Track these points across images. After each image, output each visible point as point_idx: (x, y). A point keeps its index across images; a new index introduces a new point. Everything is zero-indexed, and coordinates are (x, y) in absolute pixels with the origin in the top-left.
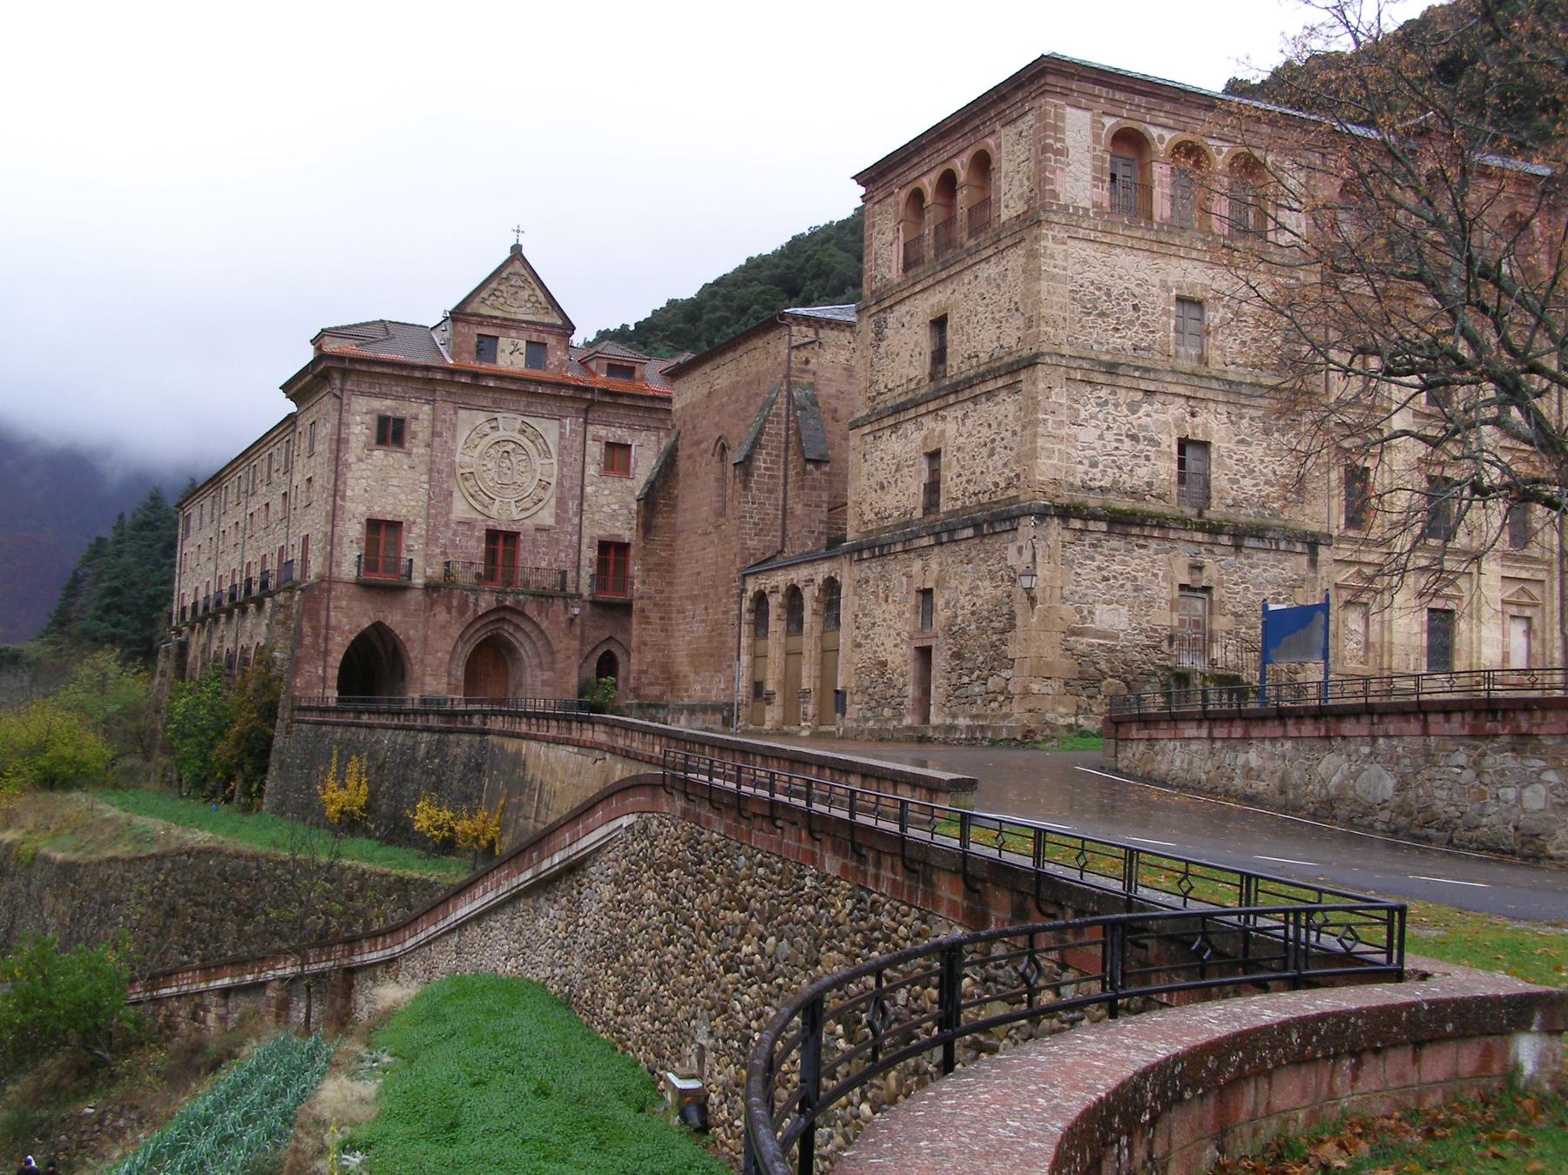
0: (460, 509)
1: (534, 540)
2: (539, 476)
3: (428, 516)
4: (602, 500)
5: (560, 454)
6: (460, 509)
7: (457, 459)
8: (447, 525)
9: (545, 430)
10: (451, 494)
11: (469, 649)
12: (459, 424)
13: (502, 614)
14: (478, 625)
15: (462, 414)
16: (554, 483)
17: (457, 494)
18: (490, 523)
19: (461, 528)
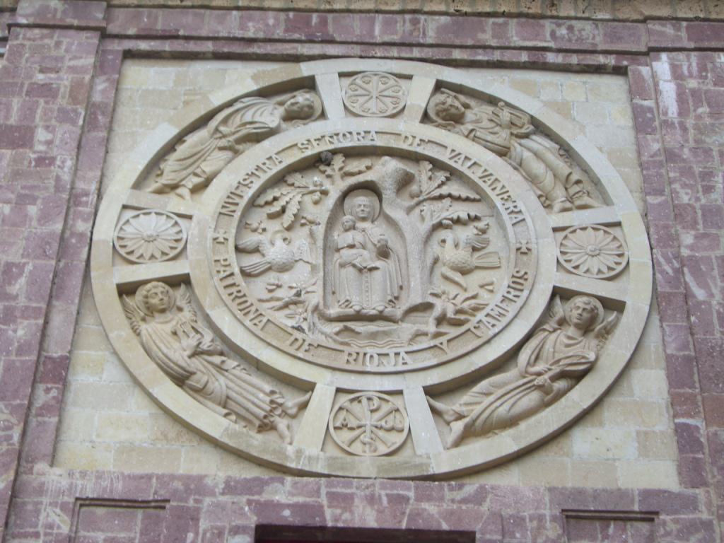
2: (549, 278)
5: (651, 184)
7: (105, 231)
9: (563, 109)
10: (55, 371)
15: (140, 76)
17: (93, 375)
18: (285, 499)
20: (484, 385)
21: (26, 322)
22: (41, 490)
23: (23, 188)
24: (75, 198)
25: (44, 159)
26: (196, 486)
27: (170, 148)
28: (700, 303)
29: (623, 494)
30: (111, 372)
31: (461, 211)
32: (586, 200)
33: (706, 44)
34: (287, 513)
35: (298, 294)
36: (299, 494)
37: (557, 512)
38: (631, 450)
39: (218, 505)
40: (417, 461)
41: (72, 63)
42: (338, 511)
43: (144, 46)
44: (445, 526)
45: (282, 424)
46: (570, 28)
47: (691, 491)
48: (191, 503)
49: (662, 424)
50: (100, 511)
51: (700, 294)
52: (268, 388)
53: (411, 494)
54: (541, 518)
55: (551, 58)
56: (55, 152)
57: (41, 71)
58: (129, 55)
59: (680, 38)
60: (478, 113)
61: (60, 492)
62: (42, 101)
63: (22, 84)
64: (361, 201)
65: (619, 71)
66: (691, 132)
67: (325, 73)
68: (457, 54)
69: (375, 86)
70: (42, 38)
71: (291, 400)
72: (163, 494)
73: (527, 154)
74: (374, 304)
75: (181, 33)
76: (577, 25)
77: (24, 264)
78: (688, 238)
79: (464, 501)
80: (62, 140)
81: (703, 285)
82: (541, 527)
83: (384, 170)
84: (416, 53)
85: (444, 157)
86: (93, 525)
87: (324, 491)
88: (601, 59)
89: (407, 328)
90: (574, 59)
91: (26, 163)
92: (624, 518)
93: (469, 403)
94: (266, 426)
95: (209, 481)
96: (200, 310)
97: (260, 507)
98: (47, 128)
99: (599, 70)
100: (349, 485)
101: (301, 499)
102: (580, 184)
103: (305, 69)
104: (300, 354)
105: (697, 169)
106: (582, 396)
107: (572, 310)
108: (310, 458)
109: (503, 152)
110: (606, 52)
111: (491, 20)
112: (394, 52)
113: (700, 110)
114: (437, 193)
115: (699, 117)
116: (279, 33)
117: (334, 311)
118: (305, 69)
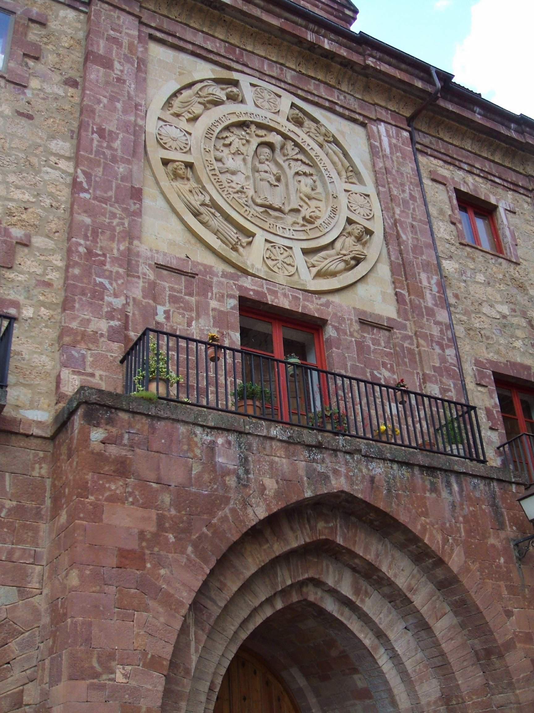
0: (162, 233)
1: (360, 345)
3: (72, 229)
4: (479, 292)
6: (162, 233)
8: (129, 261)
9: (342, 133)
10: (137, 194)
11: (223, 654)
12: (153, 69)
13: (322, 529)
14: (250, 565)
16: (377, 227)
17: (152, 202)
19: (168, 284)
20: (323, 254)
21: (123, 165)
22: (138, 255)
23: (112, 92)
24: (137, 106)
25: (121, 79)
26: (208, 270)
27: (175, 95)
28: (404, 241)
29: (381, 317)
30: (161, 203)
31: (307, 170)
32: (354, 180)
33: (399, 125)
34: (251, 293)
35: (243, 188)
36: (254, 285)
37: (357, 319)
38: (379, 298)
39: (220, 282)
40: (302, 282)
41: (127, 31)
42: (273, 298)
43: (159, 35)
44: (316, 315)
45: (241, 249)
46: (345, 97)
47: (404, 322)
48: (208, 278)
49: (390, 290)
50: (165, 272)
51: (404, 237)
52: (235, 231)
53: (301, 297)
54: (351, 320)
55: (338, 108)
56: (125, 77)
57: (112, 29)
58: (152, 37)
59: (387, 118)
60: (307, 123)
61: (147, 258)
62: (115, 46)
63: (103, 34)
64: (267, 150)
65: (363, 125)
66: (395, 163)
67: (244, 81)
68: (300, 92)
69: (266, 95)
70: (110, 11)
71: (244, 240)
72: (195, 271)
73: (330, 151)
74: (277, 203)
75: (177, 35)
76: (348, 97)
77: (118, 134)
78: (398, 211)
79: (321, 305)
80: (128, 72)
81: (405, 234)
82: (351, 324)
83: (275, 139)
84: (283, 85)
85: (299, 141)
86: (161, 277)
87: (265, 286)
88: (357, 117)
89: (290, 219)
90: (347, 113)
91: (111, 78)
92: (380, 327)
93: (322, 261)
94: (235, 249)
95: (215, 269)
96: (198, 181)
97: (240, 288)
98: (120, 62)
99: (354, 121)
100: (276, 287)
101: (256, 288)
102: (353, 173)
103: (235, 76)
104: (249, 218)
105: (399, 181)
106: (361, 270)
107: (356, 229)
108: (258, 269)
109: (321, 146)
110: (360, 114)
111: (313, 81)
112: (274, 81)
113: (398, 154)
114: (296, 157)
115: (397, 157)
116: (222, 52)
117: (259, 201)
118: (235, 76)
